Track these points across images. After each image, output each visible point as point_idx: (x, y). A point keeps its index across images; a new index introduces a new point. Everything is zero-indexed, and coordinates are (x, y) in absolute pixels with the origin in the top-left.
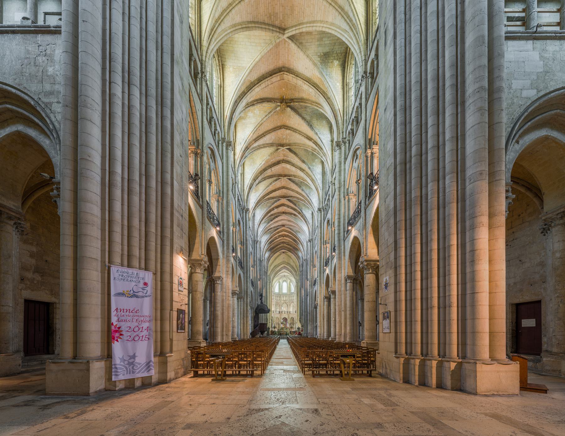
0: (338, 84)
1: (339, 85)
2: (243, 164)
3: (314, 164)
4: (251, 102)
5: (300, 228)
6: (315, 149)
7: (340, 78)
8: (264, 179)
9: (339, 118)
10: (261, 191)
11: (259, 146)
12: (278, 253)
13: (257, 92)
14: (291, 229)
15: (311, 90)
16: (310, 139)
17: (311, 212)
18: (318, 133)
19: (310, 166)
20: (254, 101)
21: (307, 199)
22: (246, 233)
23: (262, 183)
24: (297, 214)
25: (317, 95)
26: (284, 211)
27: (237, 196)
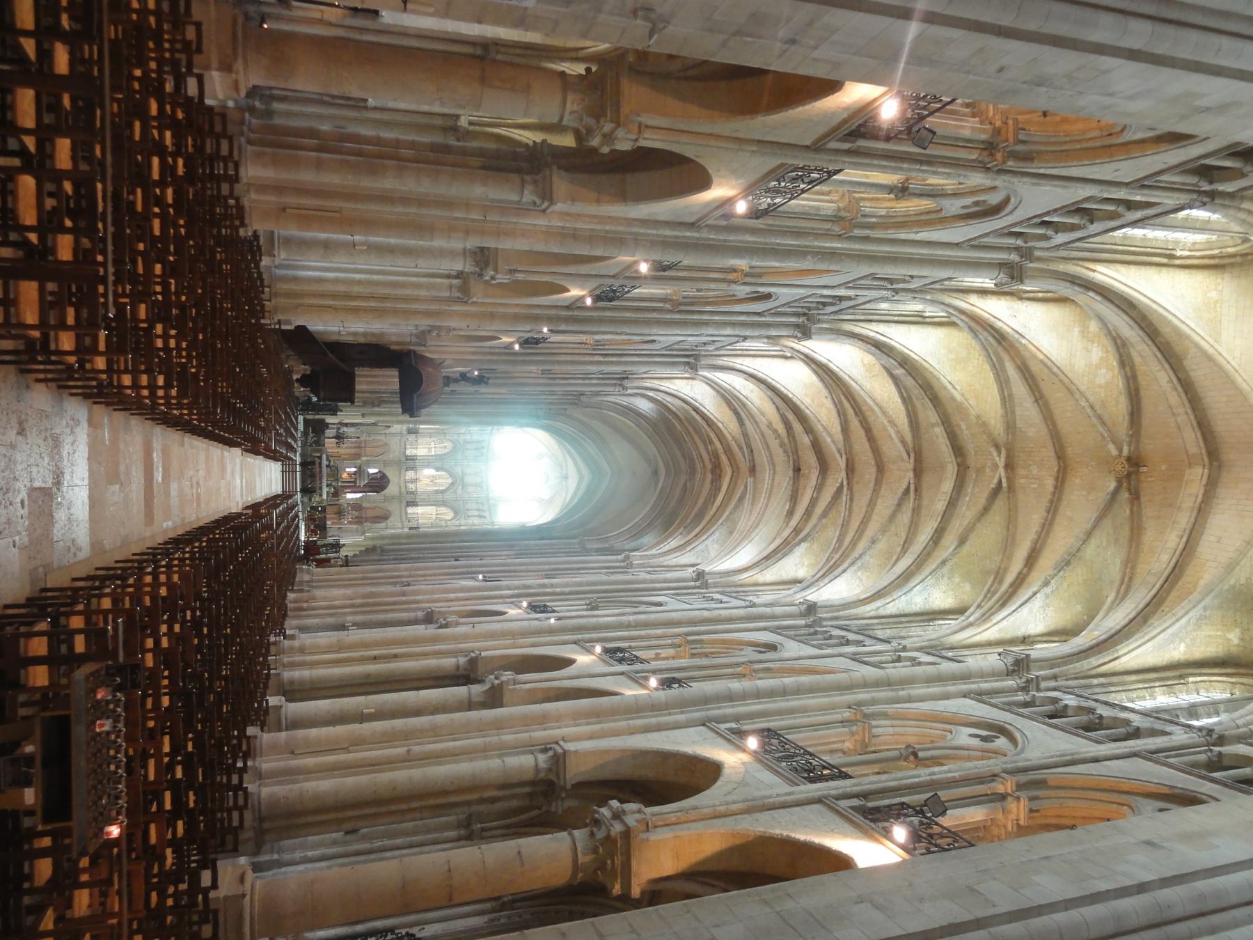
0: (1182, 647)
1: (1179, 652)
2: (953, 324)
3: (957, 580)
4: (1129, 355)
5: (746, 537)
6: (1001, 582)
7: (1200, 652)
8: (907, 400)
9: (1094, 661)
10: (867, 386)
11: (1007, 380)
12: (652, 450)
13: (1157, 378)
14: (741, 499)
15: (1165, 557)
16: (1031, 561)
17: (801, 573)
18: (1047, 590)
19: (949, 564)
20: (1133, 367)
21: (844, 556)
22: (725, 324)
23: (893, 389)
24: (793, 523)
25: (1152, 579)
26: (804, 471)
27: (851, 293)
